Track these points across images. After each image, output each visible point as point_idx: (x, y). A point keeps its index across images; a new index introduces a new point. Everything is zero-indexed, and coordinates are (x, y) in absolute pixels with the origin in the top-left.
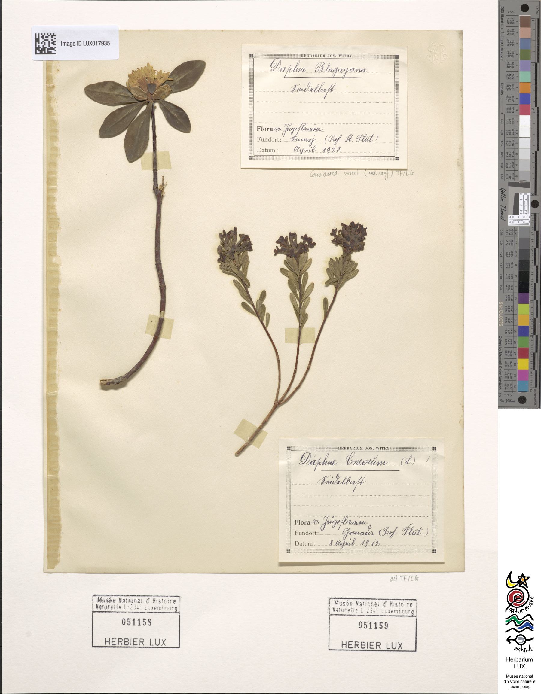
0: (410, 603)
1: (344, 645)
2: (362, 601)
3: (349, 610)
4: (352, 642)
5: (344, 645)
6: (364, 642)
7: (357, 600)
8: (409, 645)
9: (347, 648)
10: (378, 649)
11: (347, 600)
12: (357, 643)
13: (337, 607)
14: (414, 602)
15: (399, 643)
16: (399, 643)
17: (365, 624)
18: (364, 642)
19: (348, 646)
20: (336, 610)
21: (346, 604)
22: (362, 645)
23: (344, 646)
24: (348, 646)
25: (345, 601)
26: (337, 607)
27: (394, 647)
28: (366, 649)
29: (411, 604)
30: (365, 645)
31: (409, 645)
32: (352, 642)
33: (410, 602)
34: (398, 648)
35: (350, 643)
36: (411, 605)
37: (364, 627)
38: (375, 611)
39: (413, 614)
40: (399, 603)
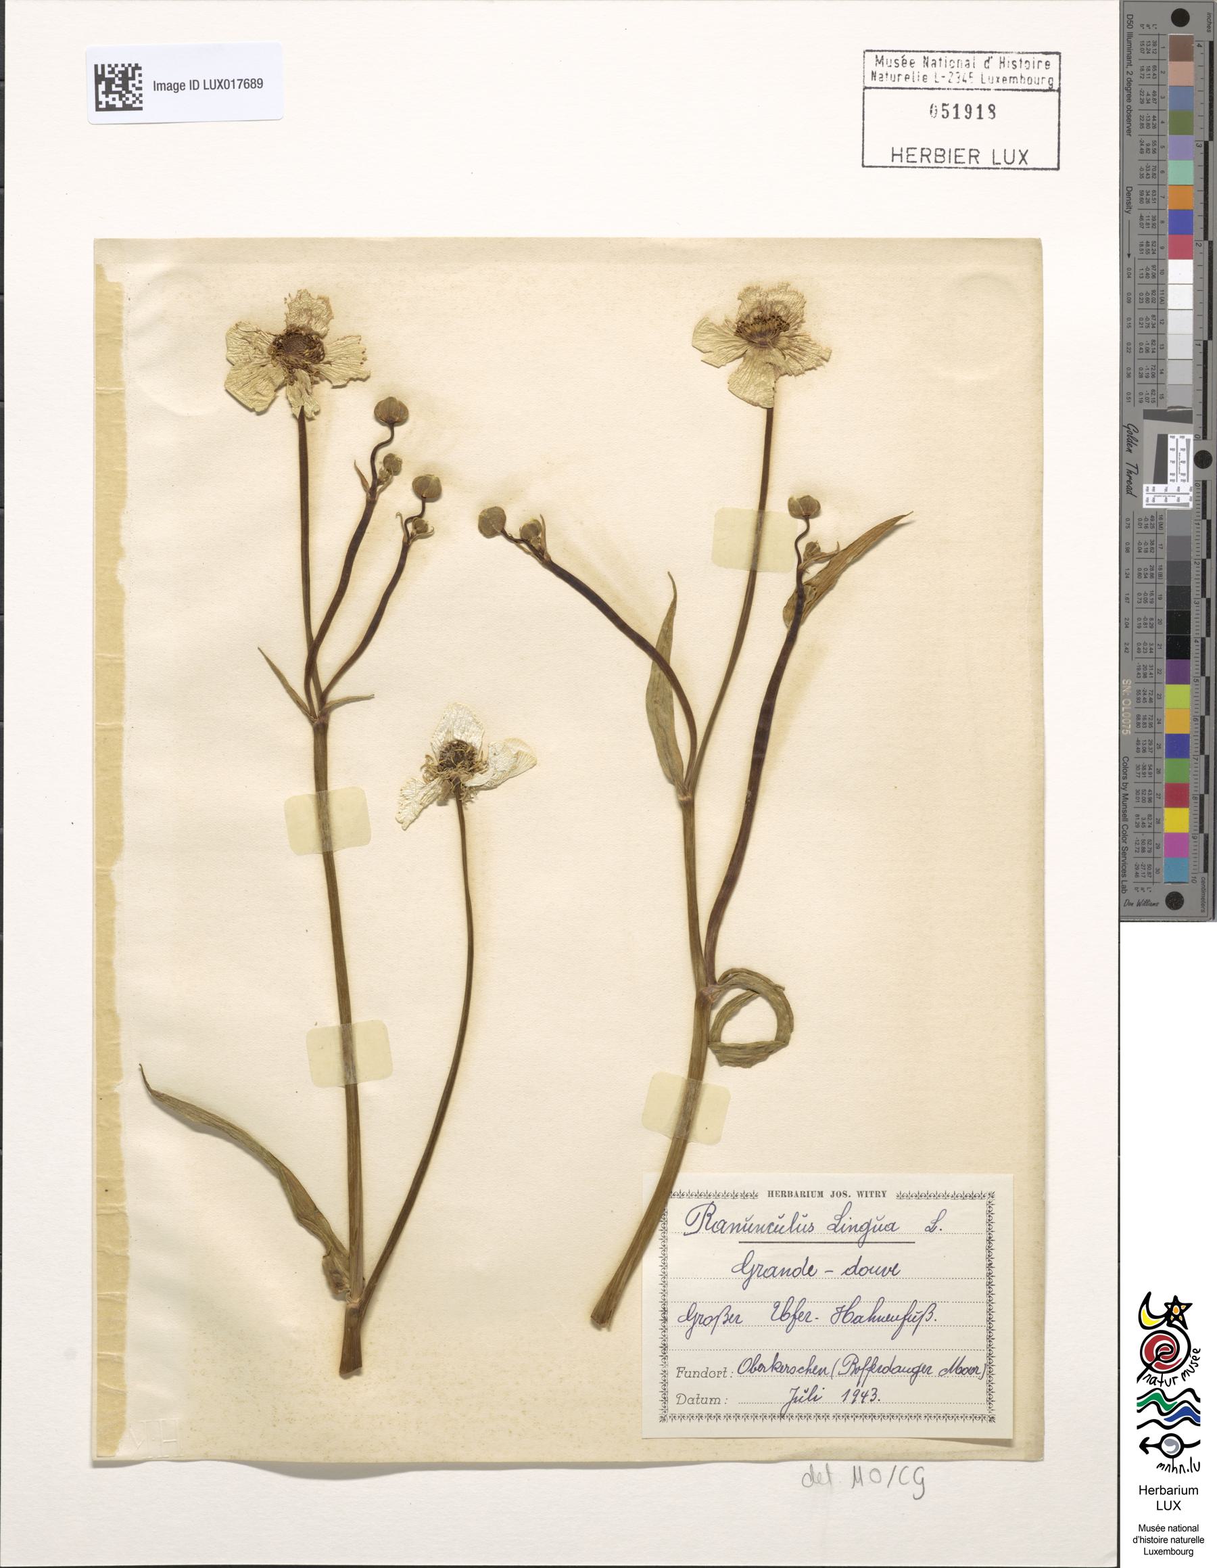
1: (896, 155)
4: (915, 148)
5: (896, 155)
6: (941, 150)
8: (1042, 155)
9: (905, 163)
10: (974, 164)
12: (926, 152)
15: (1020, 151)
16: (1020, 151)
17: (945, 107)
18: (941, 150)
19: (903, 158)
22: (936, 155)
23: (897, 159)
24: (903, 158)
27: (1009, 160)
28: (946, 164)
30: (943, 156)
31: (1042, 155)
32: (915, 148)
34: (1020, 162)
35: (911, 152)
37: (943, 116)
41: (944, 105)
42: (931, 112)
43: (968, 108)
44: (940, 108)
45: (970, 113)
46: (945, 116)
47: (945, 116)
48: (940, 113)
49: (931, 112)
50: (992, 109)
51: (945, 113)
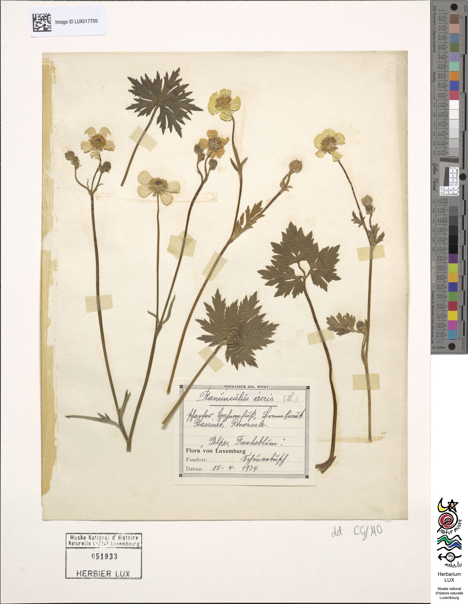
0: (135, 537)
2: (94, 535)
3: (83, 544)
7: (90, 535)
11: (81, 535)
13: (72, 541)
14: (139, 536)
17: (98, 555)
20: (71, 543)
21: (80, 538)
25: (80, 535)
26: (72, 541)
29: (137, 538)
33: (136, 536)
36: (136, 538)
38: (106, 543)
39: (139, 546)
40: (127, 537)
41: (97, 554)
42: (92, 557)
43: (107, 555)
44: (95, 555)
45: (107, 557)
46: (98, 558)
47: (98, 558)
48: (96, 557)
49: (92, 557)
50: (116, 554)
51: (98, 557)
